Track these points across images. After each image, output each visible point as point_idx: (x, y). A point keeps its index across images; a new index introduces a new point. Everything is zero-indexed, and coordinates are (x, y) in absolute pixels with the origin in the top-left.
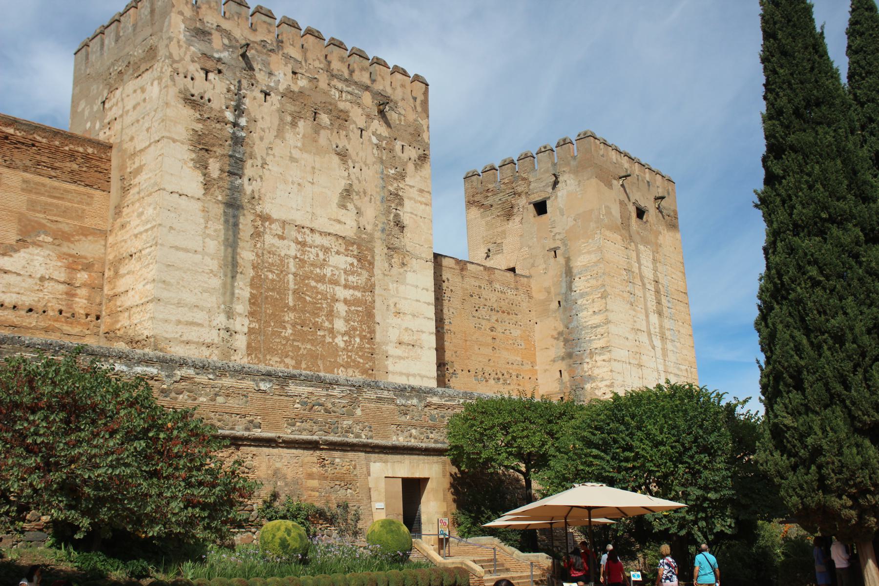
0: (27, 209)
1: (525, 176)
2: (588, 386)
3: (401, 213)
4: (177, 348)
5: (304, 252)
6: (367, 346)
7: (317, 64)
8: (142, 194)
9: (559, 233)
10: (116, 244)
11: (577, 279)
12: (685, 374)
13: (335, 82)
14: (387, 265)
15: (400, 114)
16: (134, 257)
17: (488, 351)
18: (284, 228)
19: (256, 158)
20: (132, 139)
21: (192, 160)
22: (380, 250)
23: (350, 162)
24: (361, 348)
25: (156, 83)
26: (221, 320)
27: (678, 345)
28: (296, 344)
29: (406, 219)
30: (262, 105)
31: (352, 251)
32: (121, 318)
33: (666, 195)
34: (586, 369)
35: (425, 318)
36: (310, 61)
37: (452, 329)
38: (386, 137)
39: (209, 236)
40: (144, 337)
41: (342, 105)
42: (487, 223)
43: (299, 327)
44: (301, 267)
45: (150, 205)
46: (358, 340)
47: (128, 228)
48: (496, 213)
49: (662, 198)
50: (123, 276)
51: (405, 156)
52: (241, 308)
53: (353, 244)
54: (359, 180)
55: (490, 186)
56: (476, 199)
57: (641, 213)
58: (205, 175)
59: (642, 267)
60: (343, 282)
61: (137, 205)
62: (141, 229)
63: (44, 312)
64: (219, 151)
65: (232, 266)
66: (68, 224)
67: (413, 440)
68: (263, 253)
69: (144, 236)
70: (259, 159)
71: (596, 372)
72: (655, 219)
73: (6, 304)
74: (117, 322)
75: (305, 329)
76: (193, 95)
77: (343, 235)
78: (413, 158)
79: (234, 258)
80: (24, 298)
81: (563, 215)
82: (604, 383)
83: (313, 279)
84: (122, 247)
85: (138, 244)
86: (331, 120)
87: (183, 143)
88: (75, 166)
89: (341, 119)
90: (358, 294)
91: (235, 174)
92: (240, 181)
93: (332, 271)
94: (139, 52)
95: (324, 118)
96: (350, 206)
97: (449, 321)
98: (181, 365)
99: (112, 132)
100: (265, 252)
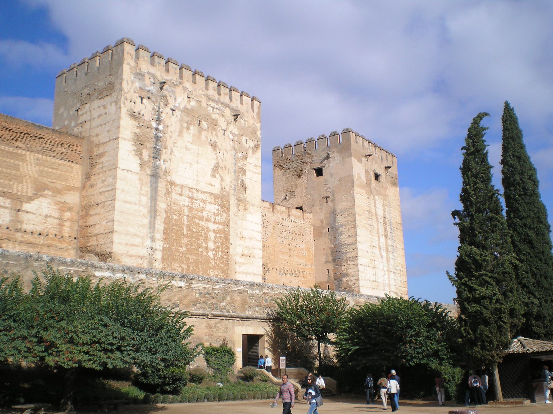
0: (39, 176)
1: (309, 152)
2: (344, 279)
3: (245, 180)
4: (126, 259)
5: (192, 203)
6: (225, 257)
7: (201, 92)
8: (105, 169)
9: (330, 188)
10: (86, 196)
11: (339, 216)
12: (399, 272)
13: (210, 103)
14: (236, 209)
15: (245, 120)
16: (99, 206)
17: (286, 257)
18: (182, 189)
19: (167, 149)
20: (97, 135)
21: (134, 150)
22: (233, 201)
23: (217, 149)
24: (222, 258)
25: (113, 104)
26: (148, 243)
27: (395, 254)
28: (187, 256)
29: (247, 183)
30: (171, 117)
31: (218, 202)
32: (91, 240)
33: (391, 166)
34: (343, 269)
35: (256, 240)
36: (197, 90)
37: (267, 245)
38: (237, 134)
39: (142, 194)
40: (107, 252)
41: (214, 116)
42: (286, 179)
43: (189, 247)
44: (190, 212)
45: (110, 176)
46: (220, 253)
47: (95, 187)
48: (292, 173)
49: (390, 167)
50: (92, 215)
51: (247, 146)
52: (159, 236)
53: (219, 197)
54: (222, 160)
55: (289, 157)
56: (279, 164)
57: (377, 176)
58: (141, 159)
59: (377, 209)
60: (213, 220)
61: (101, 175)
62: (105, 190)
63: (47, 235)
64: (148, 145)
65: (154, 212)
66: (59, 184)
67: (256, 314)
68: (171, 204)
69: (106, 194)
70: (169, 149)
71: (349, 271)
72: (385, 179)
73: (27, 231)
74: (89, 242)
75: (192, 247)
76: (134, 112)
77: (213, 193)
78: (251, 147)
79: (155, 207)
80: (37, 227)
81: (332, 177)
82: (354, 278)
83: (197, 218)
84: (91, 199)
85: (102, 198)
86: (208, 125)
87: (129, 141)
88: (64, 150)
89: (214, 124)
90: (221, 227)
91: (156, 158)
92: (158, 163)
93: (207, 214)
94: (101, 84)
95: (204, 124)
96: (217, 176)
97: (266, 239)
98: (139, 273)
99: (83, 129)
100: (172, 203)
